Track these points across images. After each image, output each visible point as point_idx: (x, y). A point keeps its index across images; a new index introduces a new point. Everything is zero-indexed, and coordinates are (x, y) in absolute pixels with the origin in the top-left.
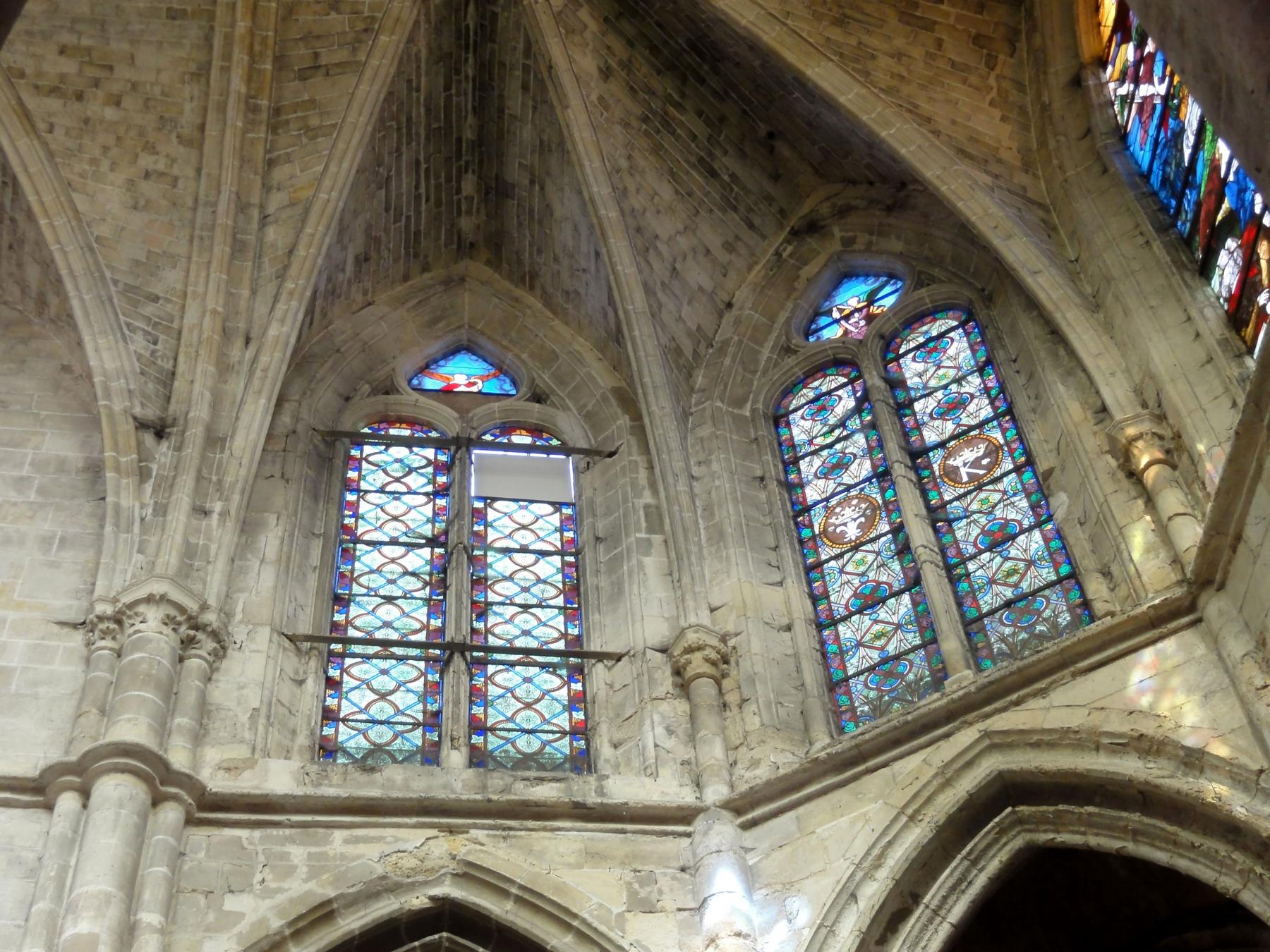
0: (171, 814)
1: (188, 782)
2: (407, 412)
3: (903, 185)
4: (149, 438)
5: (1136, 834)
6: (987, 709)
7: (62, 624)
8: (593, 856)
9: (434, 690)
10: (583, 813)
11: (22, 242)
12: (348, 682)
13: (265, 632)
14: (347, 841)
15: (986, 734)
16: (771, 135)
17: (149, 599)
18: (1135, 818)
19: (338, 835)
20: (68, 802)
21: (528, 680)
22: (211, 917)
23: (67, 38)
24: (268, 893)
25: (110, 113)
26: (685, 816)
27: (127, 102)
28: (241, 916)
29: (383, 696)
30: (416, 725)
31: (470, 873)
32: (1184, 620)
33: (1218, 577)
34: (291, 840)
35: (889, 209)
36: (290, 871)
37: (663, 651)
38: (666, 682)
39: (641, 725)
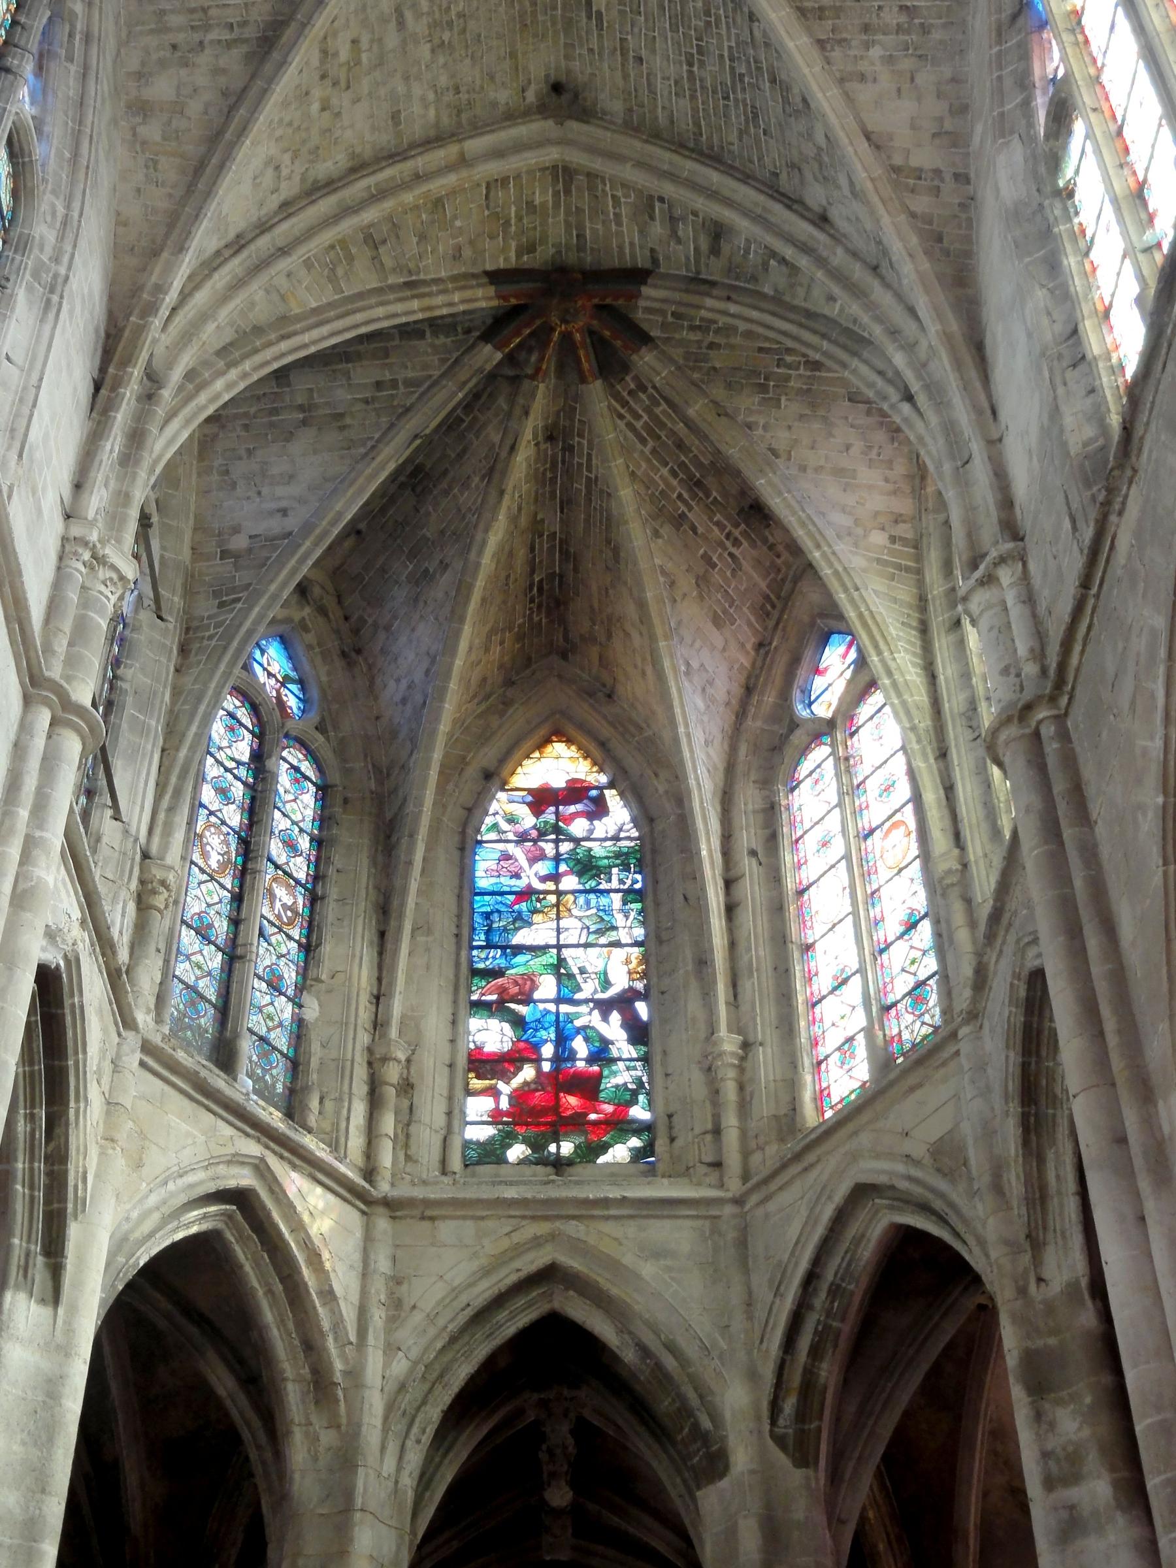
3: (359, 651)
5: (270, 1292)
6: (272, 1145)
15: (262, 1160)
16: (359, 532)
18: (279, 1288)
23: (364, 44)
25: (315, 107)
27: (326, 114)
32: (362, 1206)
33: (398, 1214)
35: (344, 654)
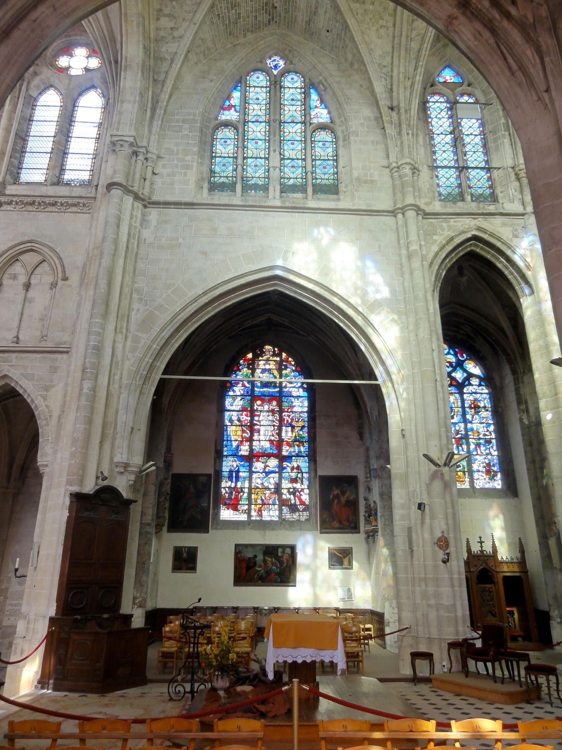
0: (420, 217)
1: (423, 211)
2: (438, 91)
4: (390, 110)
7: (383, 167)
8: (504, 224)
9: (459, 177)
10: (502, 214)
11: (346, 47)
12: (440, 176)
13: (425, 166)
14: (454, 222)
17: (406, 163)
19: (452, 220)
20: (400, 216)
21: (478, 173)
22: (431, 241)
24: (441, 235)
25: (371, 7)
26: (523, 215)
28: (437, 240)
29: (448, 179)
30: (456, 187)
31: (479, 229)
34: (442, 222)
36: (444, 230)
37: (513, 168)
38: (513, 177)
39: (508, 188)
